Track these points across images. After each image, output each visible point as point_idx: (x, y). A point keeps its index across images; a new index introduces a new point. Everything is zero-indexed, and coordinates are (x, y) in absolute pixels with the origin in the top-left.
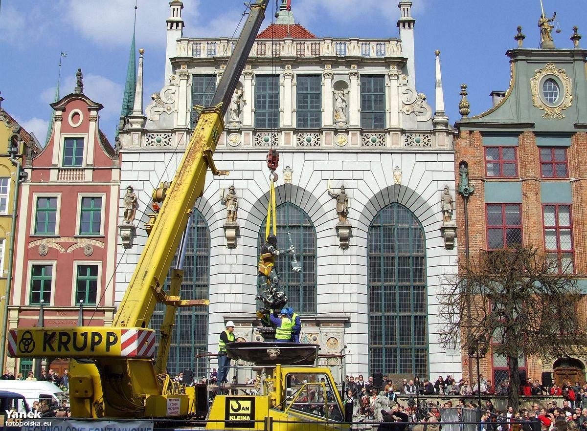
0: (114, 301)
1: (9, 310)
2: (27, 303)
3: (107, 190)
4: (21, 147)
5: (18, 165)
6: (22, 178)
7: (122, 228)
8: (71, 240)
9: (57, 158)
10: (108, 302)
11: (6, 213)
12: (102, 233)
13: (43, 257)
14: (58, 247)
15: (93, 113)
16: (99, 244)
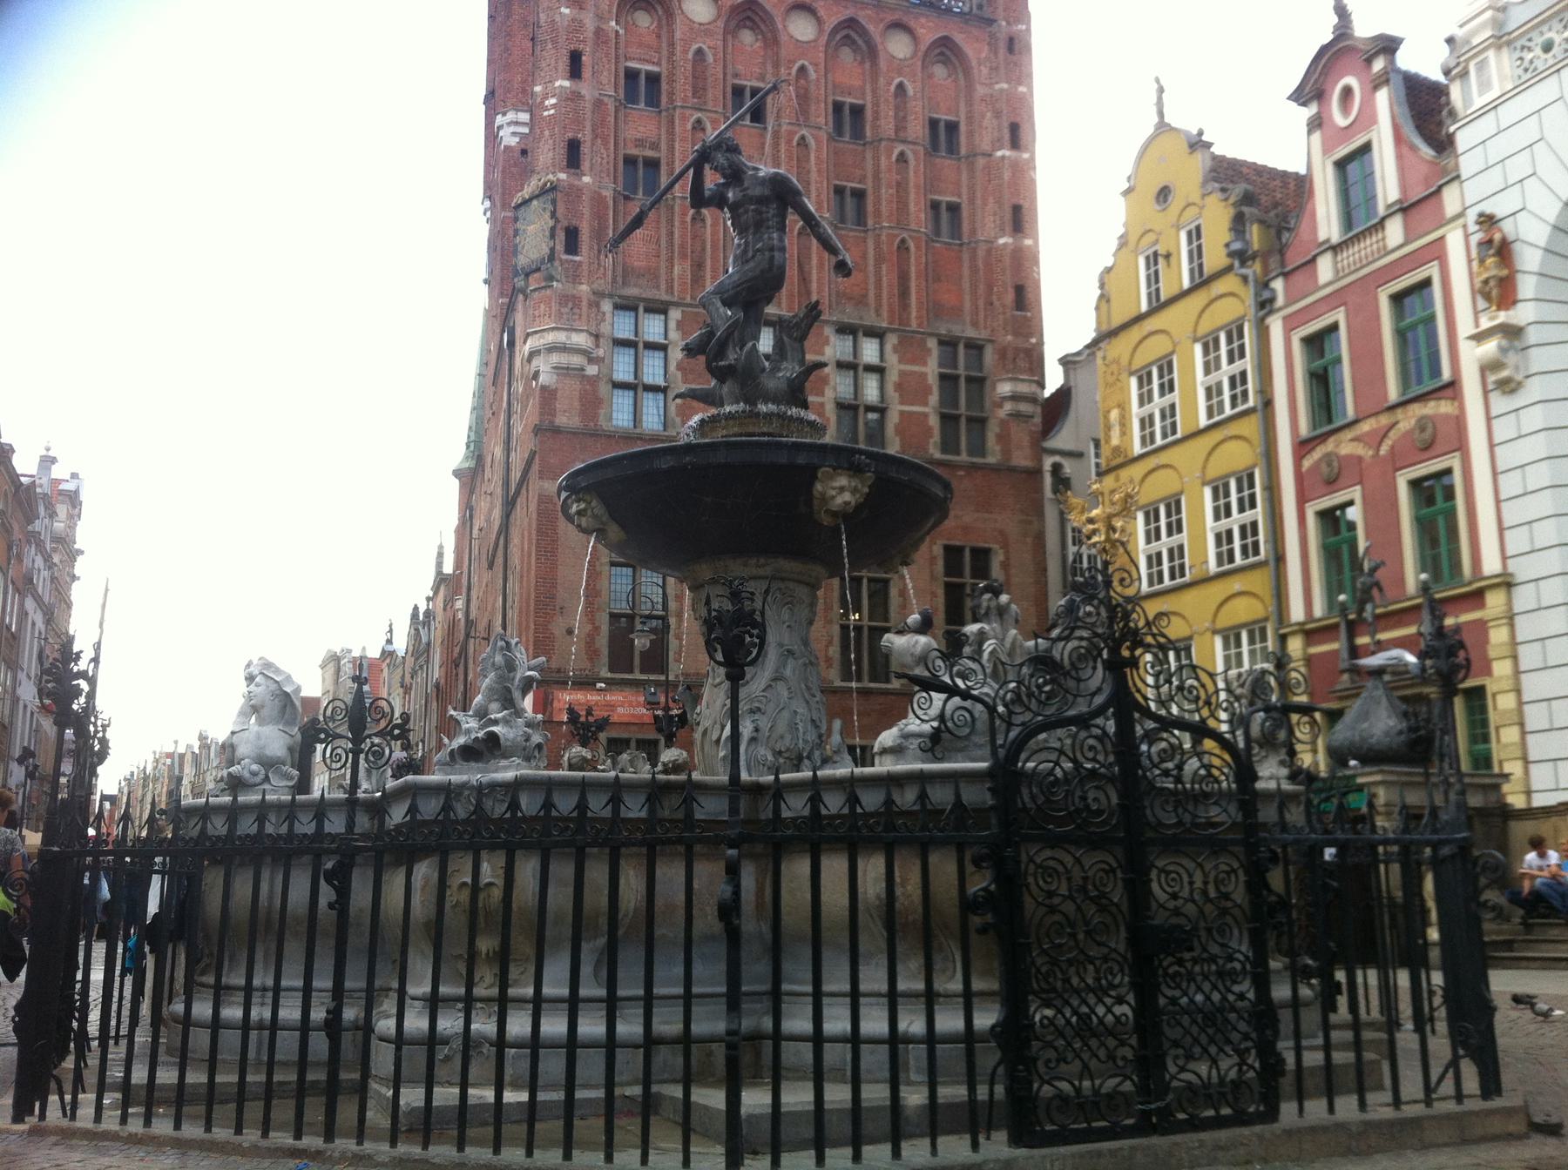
0: (1504, 558)
1: (1283, 639)
2: (1318, 611)
3: (1437, 251)
4: (1255, 234)
5: (1251, 278)
6: (1265, 305)
7: (1479, 338)
8: (1384, 420)
9: (1326, 219)
10: (1491, 564)
11: (1251, 403)
12: (1446, 374)
13: (1332, 483)
14: (1359, 450)
15: (1379, 65)
16: (1444, 407)
